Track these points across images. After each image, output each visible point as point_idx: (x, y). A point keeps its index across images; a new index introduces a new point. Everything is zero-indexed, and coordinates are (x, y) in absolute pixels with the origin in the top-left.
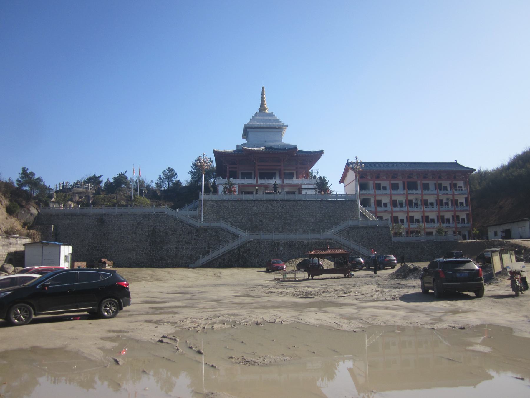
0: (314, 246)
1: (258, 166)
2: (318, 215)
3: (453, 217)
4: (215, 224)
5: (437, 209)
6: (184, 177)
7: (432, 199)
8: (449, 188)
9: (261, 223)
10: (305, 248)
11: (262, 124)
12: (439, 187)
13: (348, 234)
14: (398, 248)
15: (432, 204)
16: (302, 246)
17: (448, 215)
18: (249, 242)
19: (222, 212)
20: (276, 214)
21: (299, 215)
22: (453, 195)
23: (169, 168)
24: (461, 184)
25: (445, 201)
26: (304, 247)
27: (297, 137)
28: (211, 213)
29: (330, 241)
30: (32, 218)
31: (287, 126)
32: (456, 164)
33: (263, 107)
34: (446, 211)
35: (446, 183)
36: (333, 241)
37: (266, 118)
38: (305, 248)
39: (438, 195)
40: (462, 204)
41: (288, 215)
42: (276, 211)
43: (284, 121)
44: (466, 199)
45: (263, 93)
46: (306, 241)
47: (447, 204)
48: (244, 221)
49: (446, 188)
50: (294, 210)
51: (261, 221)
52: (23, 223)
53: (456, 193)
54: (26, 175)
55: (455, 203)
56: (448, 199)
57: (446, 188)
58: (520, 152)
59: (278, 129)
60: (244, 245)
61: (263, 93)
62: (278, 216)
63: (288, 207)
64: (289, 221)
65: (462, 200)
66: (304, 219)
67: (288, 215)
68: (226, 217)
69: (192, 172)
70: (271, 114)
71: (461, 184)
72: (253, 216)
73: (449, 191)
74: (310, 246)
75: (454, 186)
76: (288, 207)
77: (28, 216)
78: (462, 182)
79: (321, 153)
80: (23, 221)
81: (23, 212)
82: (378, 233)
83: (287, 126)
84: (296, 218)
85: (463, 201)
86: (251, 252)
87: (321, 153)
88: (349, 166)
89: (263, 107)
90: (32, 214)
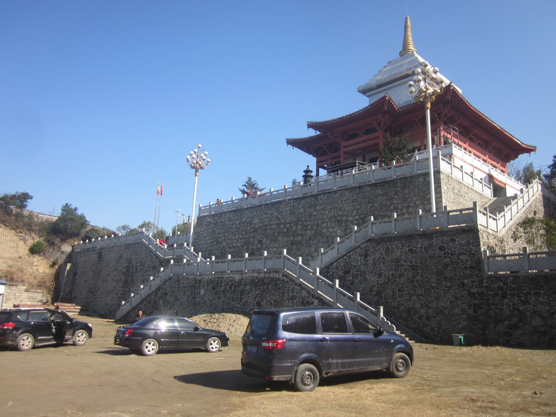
0: (248, 287)
1: (345, 147)
2: (351, 218)
9: (259, 246)
10: (235, 291)
13: (366, 256)
14: (504, 297)
16: (231, 287)
18: (169, 280)
19: (218, 231)
20: (282, 226)
21: (318, 223)
26: (233, 288)
28: (205, 235)
29: (276, 275)
30: (64, 257)
36: (281, 276)
37: (398, 65)
38: (235, 291)
41: (299, 227)
42: (283, 221)
46: (237, 277)
48: (239, 245)
50: (310, 215)
51: (260, 242)
52: (53, 262)
54: (68, 211)
60: (162, 285)
62: (285, 230)
63: (302, 211)
64: (300, 238)
66: (325, 231)
67: (299, 227)
68: (220, 240)
72: (252, 235)
74: (241, 287)
76: (302, 211)
77: (58, 255)
80: (52, 260)
81: (51, 250)
82: (441, 248)
84: (311, 230)
86: (167, 296)
90: (63, 252)
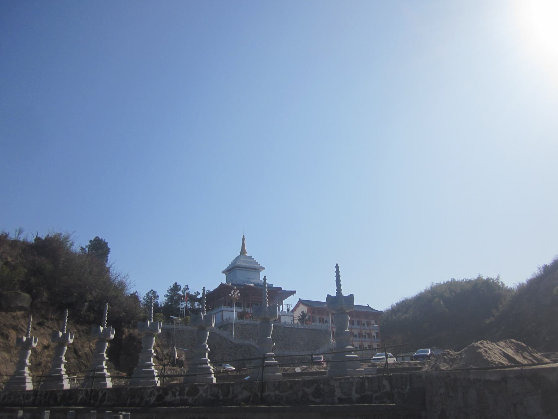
3: (369, 346)
4: (247, 342)
5: (360, 339)
6: (162, 300)
7: (356, 332)
8: (366, 325)
11: (247, 264)
12: (359, 323)
15: (356, 336)
17: (366, 345)
22: (370, 330)
23: (152, 290)
24: (373, 322)
25: (364, 334)
27: (273, 277)
31: (264, 268)
32: (368, 307)
33: (243, 251)
34: (365, 341)
35: (364, 321)
39: (361, 330)
40: (374, 337)
43: (262, 264)
44: (377, 333)
45: (243, 240)
47: (365, 337)
49: (364, 324)
53: (371, 328)
55: (369, 335)
56: (366, 333)
57: (364, 324)
58: (399, 302)
59: (257, 269)
61: (243, 240)
65: (374, 334)
69: (168, 296)
70: (251, 257)
71: (373, 322)
73: (366, 327)
75: (368, 324)
78: (374, 321)
79: (294, 292)
83: (264, 268)
85: (375, 335)
87: (294, 292)
88: (301, 302)
89: (243, 251)
